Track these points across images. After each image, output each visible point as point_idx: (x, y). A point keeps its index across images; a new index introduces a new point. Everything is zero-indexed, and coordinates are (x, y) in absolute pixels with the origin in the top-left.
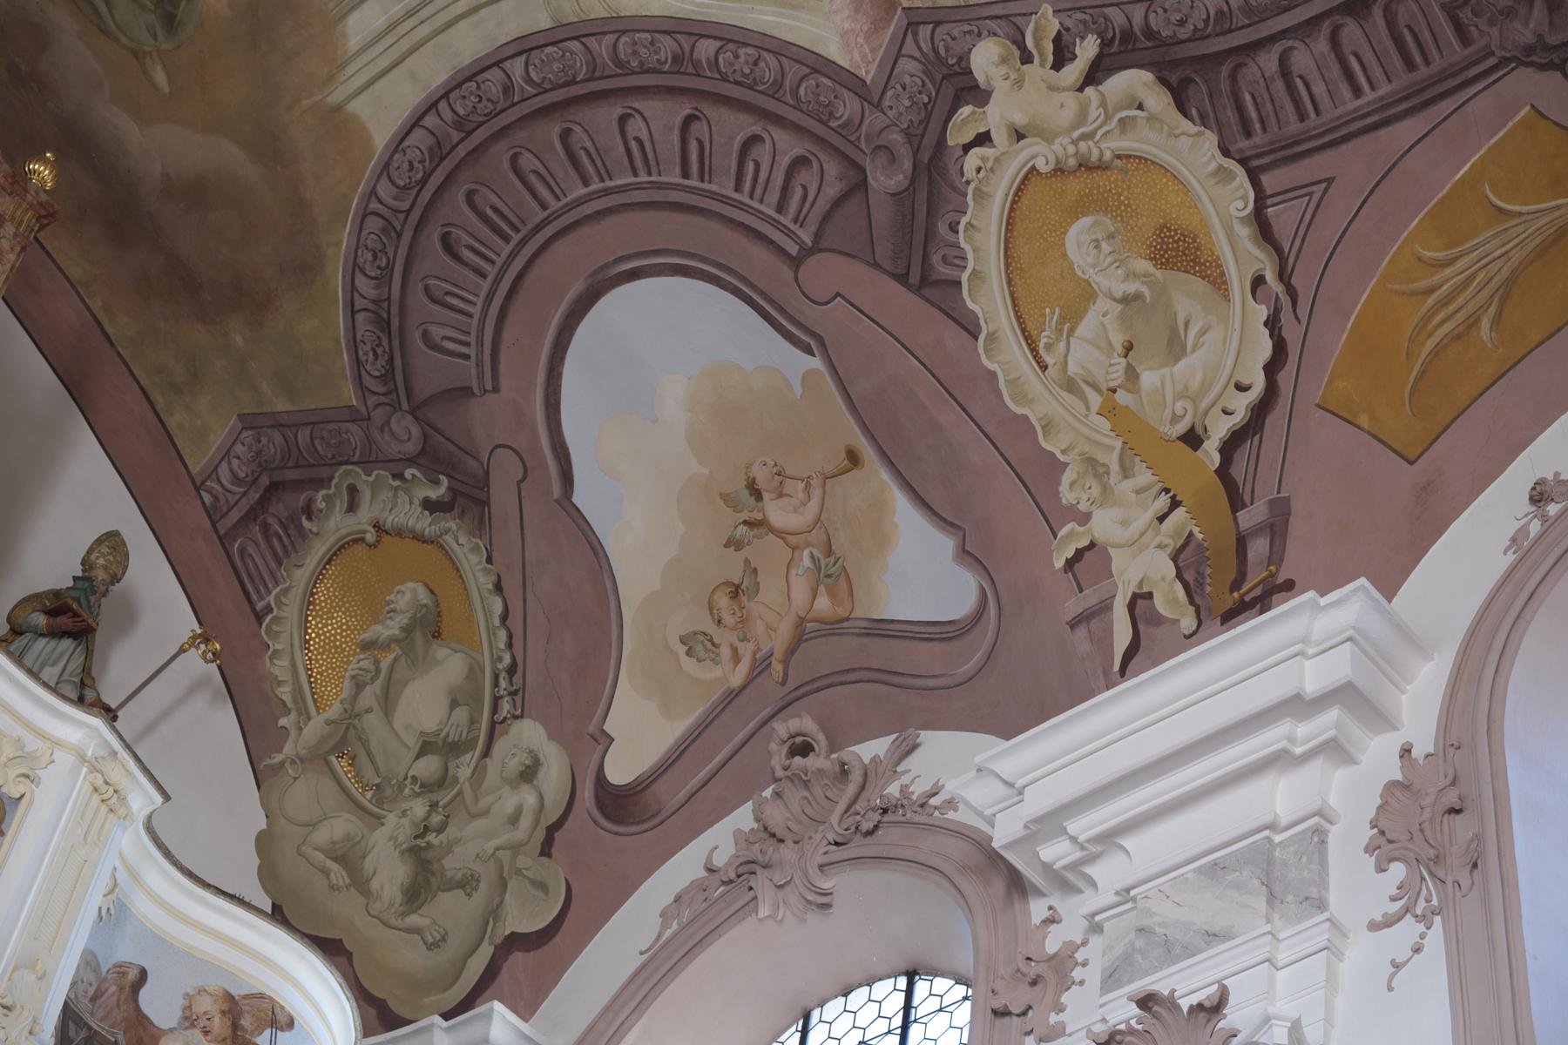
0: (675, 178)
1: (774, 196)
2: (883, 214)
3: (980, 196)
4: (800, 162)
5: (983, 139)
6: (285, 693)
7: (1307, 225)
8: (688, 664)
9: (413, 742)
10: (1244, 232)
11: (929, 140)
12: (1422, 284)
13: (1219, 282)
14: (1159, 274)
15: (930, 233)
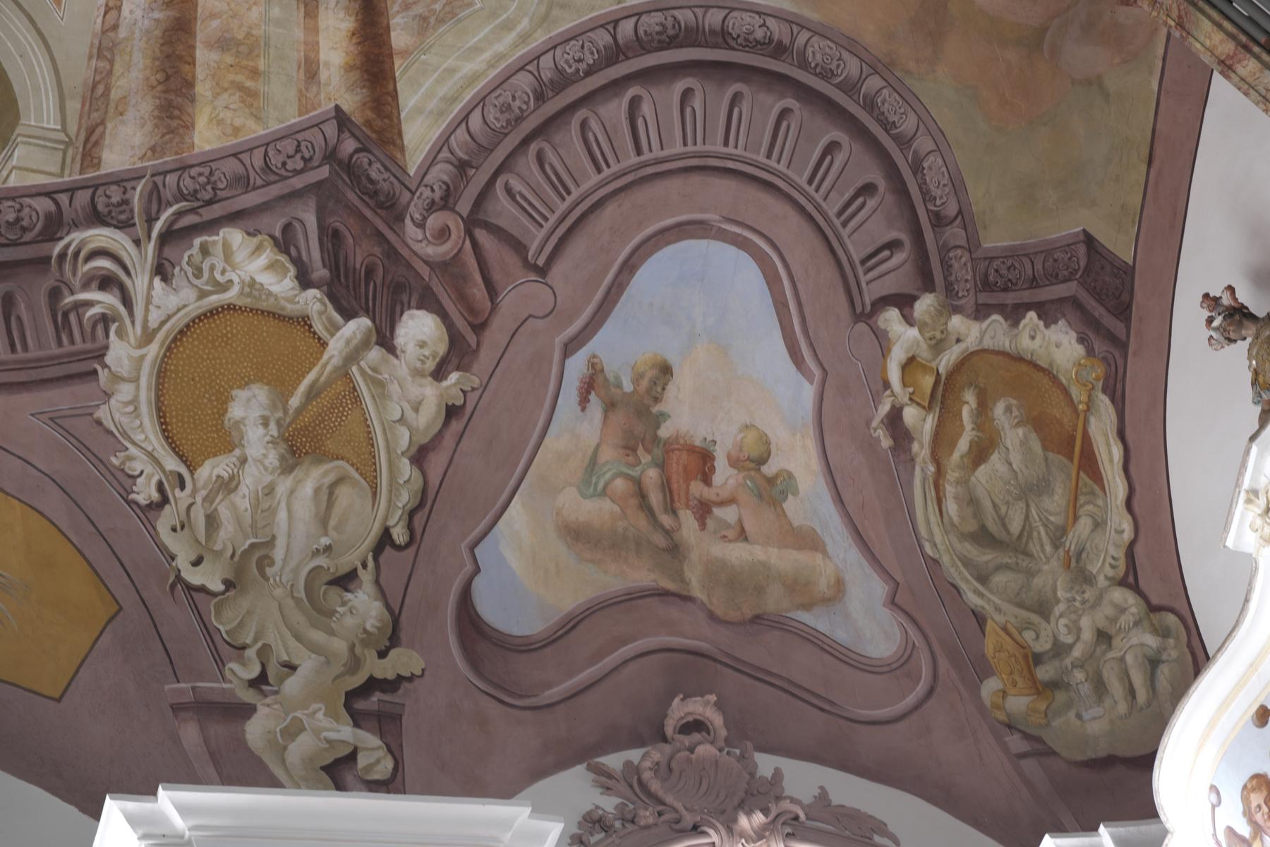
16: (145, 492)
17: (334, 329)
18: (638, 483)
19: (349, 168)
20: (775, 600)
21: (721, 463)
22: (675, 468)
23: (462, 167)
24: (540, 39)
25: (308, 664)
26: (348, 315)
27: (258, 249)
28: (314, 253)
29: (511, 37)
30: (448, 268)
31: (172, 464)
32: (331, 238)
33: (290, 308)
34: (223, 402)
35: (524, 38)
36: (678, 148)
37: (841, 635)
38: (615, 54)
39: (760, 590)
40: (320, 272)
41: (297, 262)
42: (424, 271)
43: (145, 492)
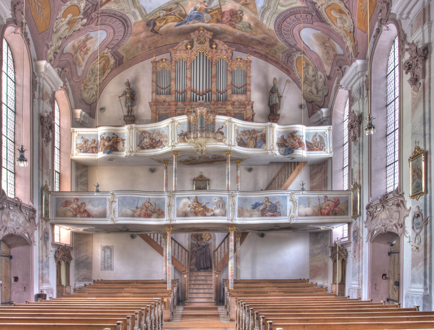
0: (297, 21)
1: (306, 19)
2: (316, 17)
3: (323, 12)
4: (306, 16)
5: (319, 7)
6: (299, 77)
7: (349, 5)
8: (328, 61)
9: (311, 76)
10: (345, 8)
11: (315, 9)
12: (361, 9)
13: (346, 14)
14: (341, 14)
15: (321, 17)
16: (57, 17)
17: (81, 15)
18: (80, 44)
19: (97, 5)
20: (77, 63)
21: (86, 48)
22: (83, 46)
23: (102, 13)
24: (119, 11)
25: (54, 46)
26: (83, 15)
27: (84, 4)
28: (87, 8)
29: (117, 8)
30: (92, 18)
31: (61, 16)
32: (89, 8)
33: (81, 11)
34: (69, 14)
35: (118, 9)
36: (114, 26)
37: (78, 70)
38: (120, 17)
39: (77, 61)
40: (85, 10)
41: (85, 8)
42: (91, 17)
43: (57, 17)
